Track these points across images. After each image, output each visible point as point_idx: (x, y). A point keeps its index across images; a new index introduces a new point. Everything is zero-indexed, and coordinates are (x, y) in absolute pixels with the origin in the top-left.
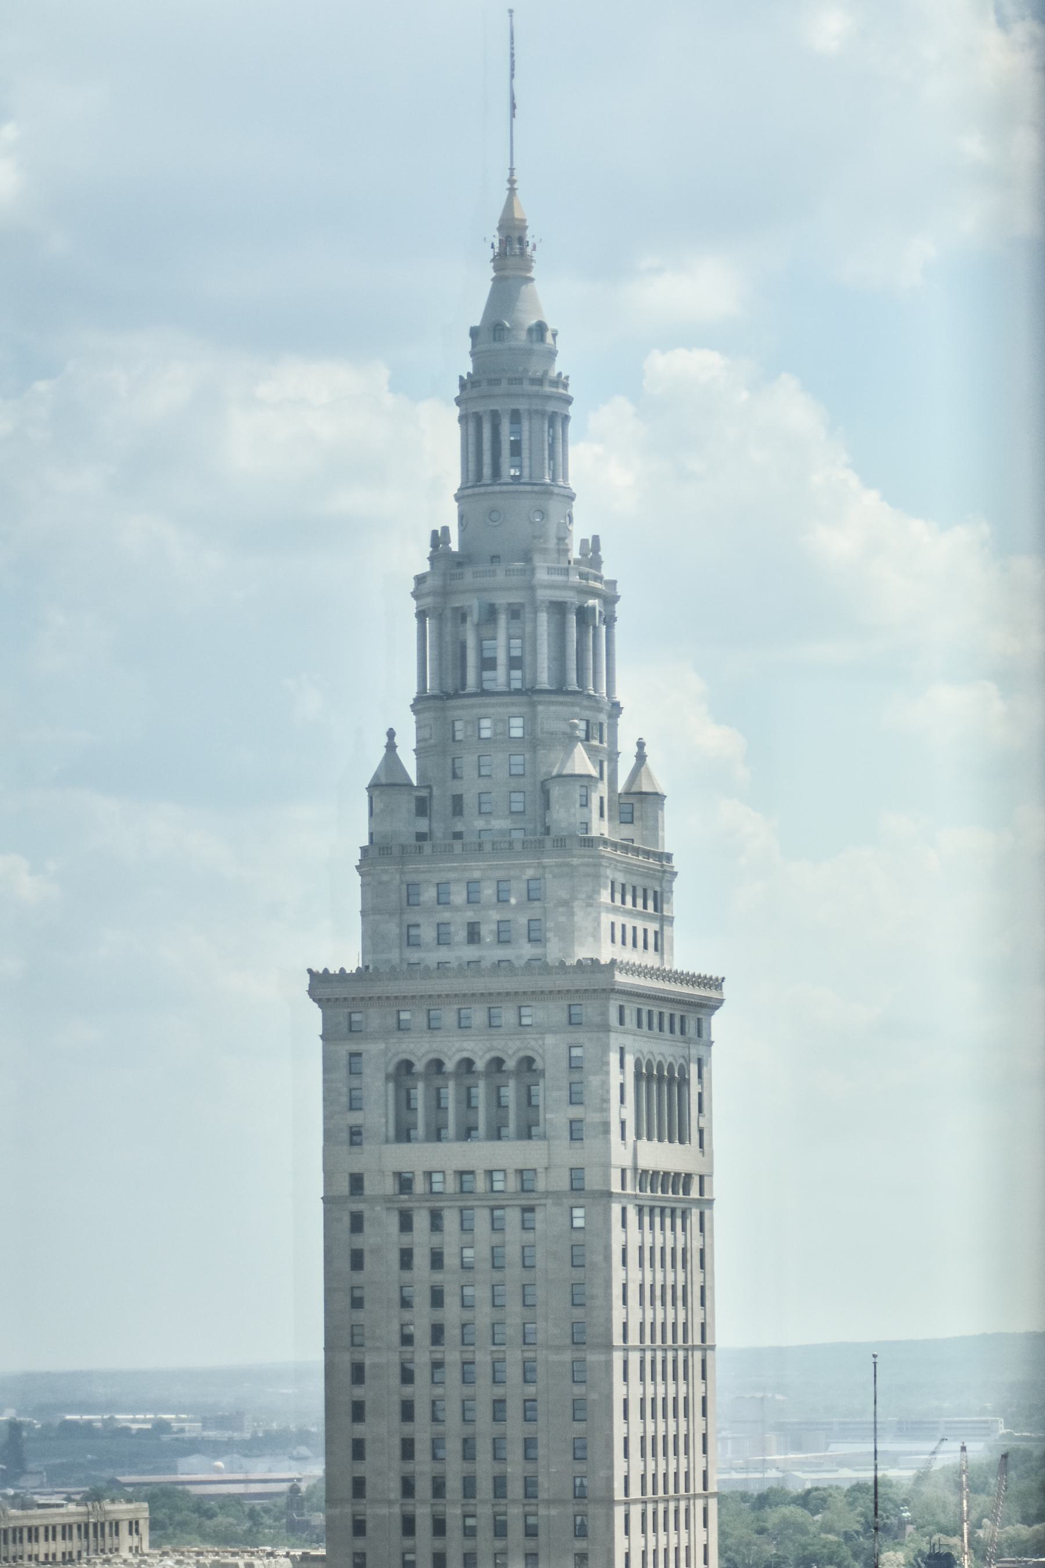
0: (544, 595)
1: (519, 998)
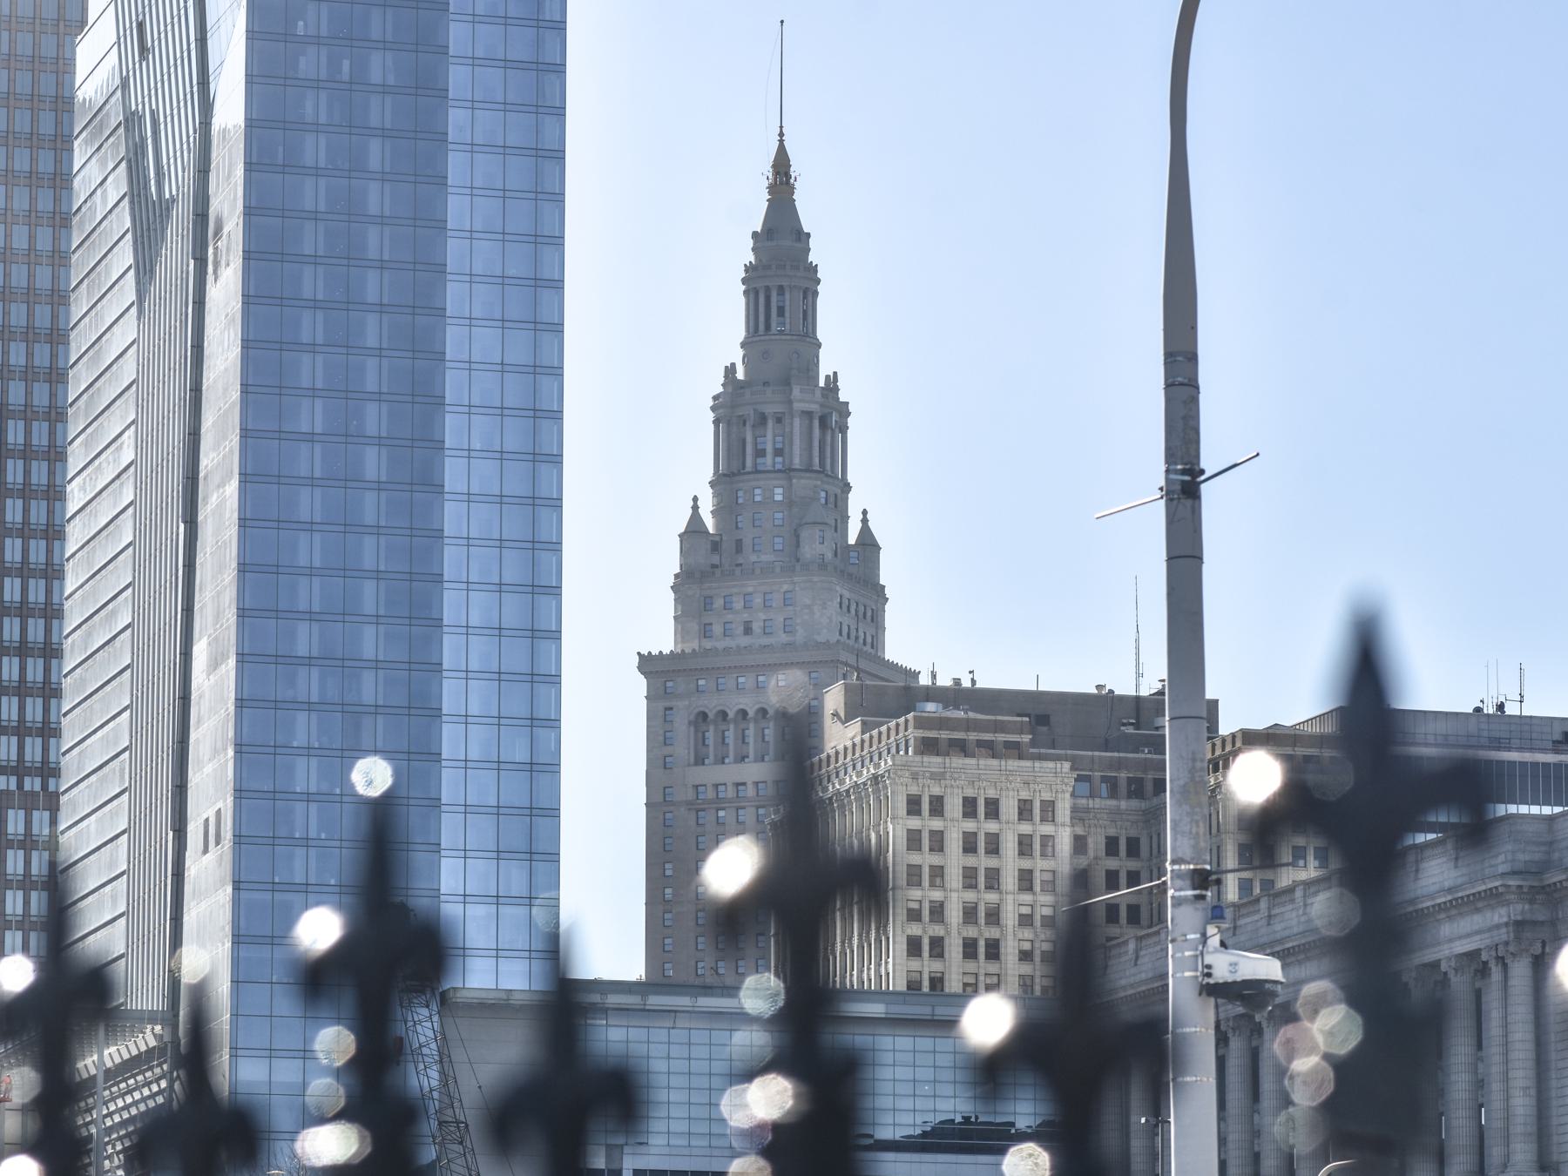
0: (797, 406)
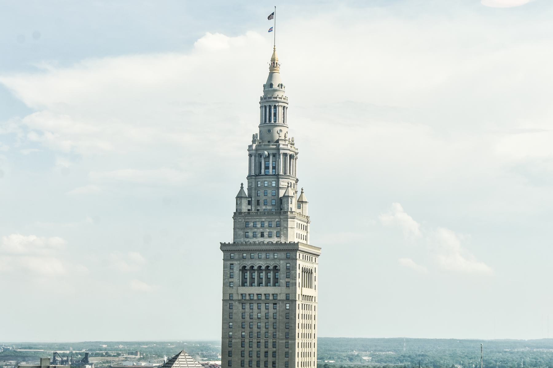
0: (282, 152)
1: (274, 251)
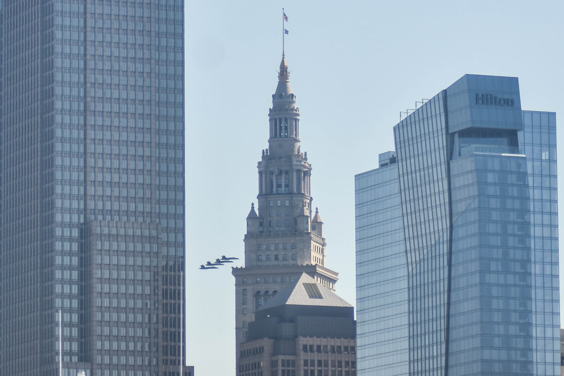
0: (295, 167)
